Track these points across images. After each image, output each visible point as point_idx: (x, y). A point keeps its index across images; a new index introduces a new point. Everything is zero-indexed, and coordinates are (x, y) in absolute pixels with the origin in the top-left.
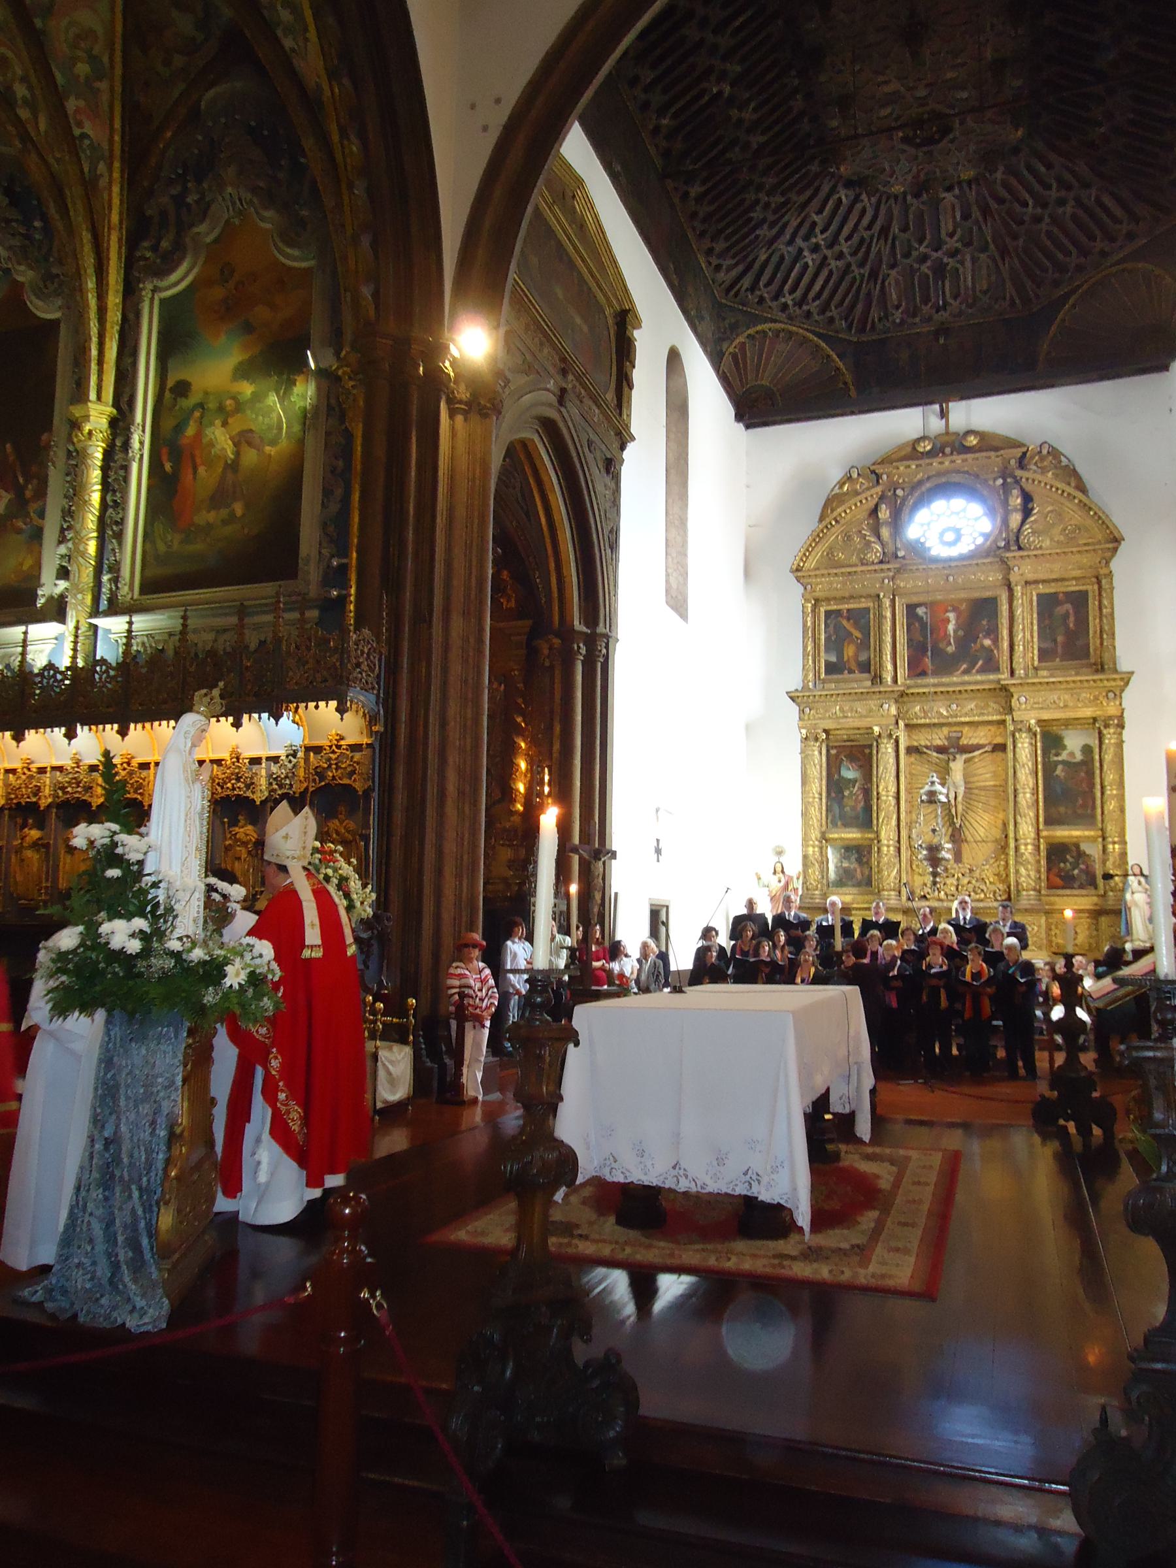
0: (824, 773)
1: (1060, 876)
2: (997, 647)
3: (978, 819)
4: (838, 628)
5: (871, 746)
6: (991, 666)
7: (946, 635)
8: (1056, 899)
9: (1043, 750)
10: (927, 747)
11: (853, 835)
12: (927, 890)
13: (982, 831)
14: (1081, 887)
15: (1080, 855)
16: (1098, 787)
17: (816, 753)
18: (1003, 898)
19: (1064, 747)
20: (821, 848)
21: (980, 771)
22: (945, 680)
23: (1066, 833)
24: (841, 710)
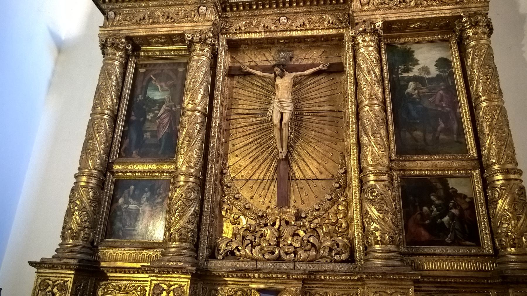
1: (426, 227)
5: (186, 64)
9: (390, 65)
10: (251, 67)
14: (455, 242)
15: (451, 195)
18: (343, 257)
19: (416, 62)
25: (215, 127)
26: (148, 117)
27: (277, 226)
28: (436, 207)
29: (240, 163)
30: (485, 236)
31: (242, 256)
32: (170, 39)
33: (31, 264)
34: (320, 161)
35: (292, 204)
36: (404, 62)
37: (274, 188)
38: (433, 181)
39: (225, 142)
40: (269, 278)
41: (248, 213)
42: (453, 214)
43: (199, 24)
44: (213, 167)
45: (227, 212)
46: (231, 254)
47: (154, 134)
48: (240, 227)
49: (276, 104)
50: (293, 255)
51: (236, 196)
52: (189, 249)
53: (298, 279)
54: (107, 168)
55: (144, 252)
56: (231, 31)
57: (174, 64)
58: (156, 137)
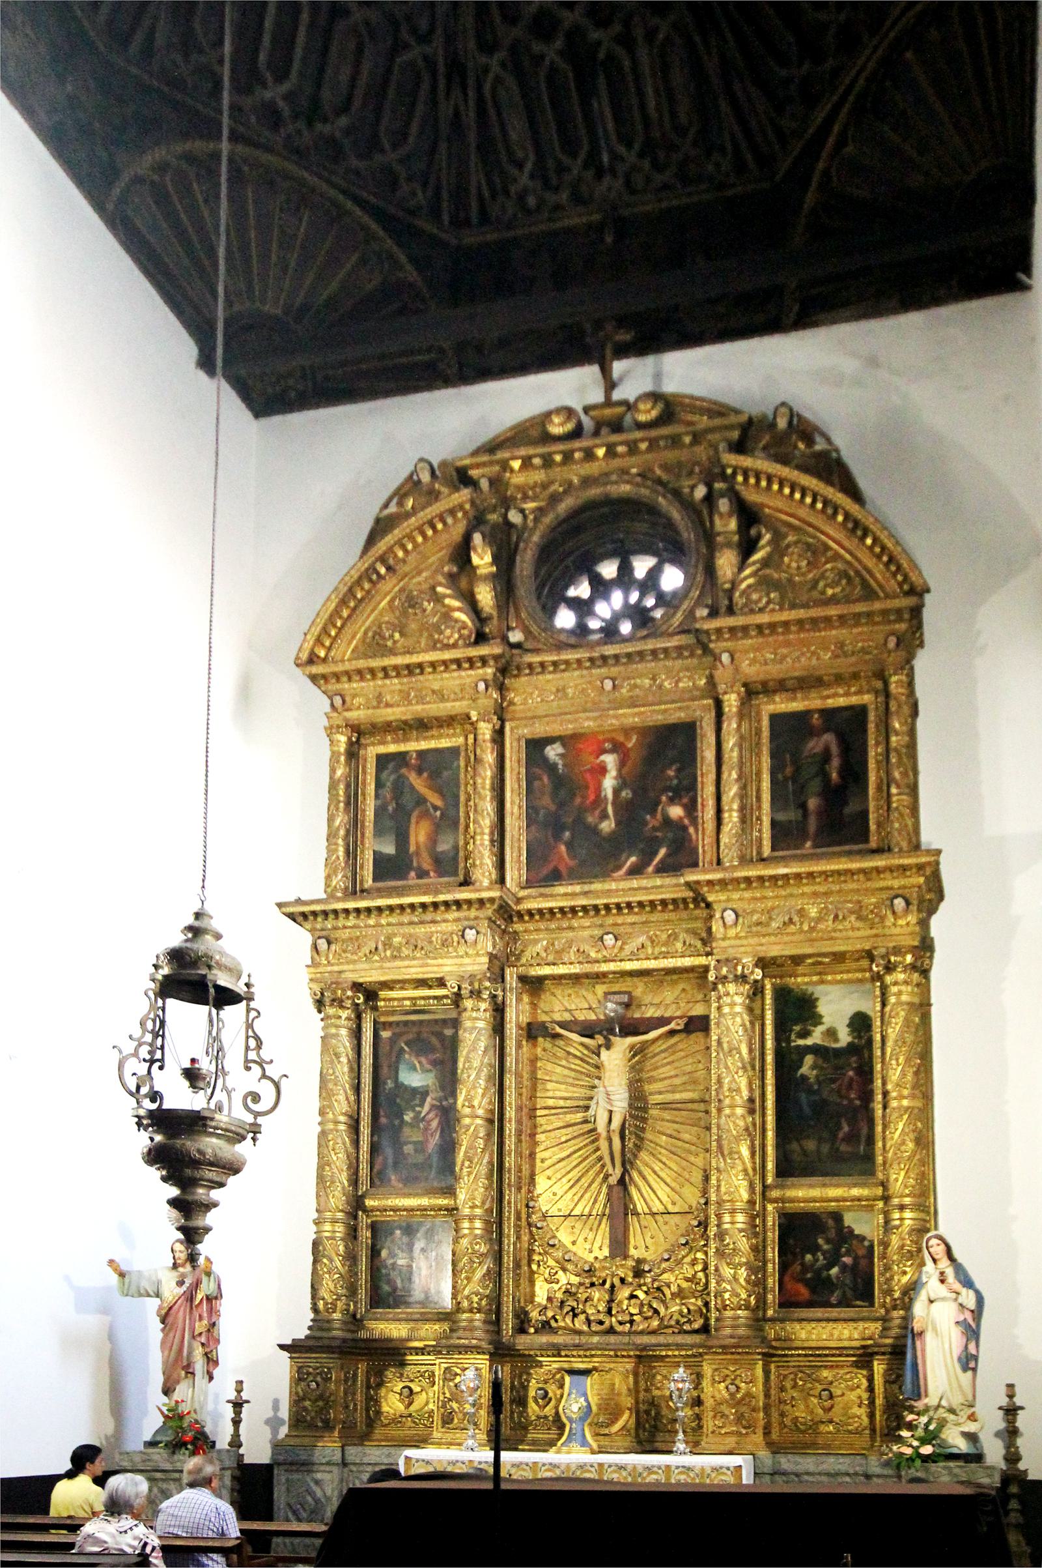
1: (807, 1283)
2: (694, 821)
4: (400, 787)
5: (456, 1023)
6: (682, 855)
7: (599, 800)
8: (797, 1326)
10: (562, 1025)
15: (845, 1236)
16: (879, 1097)
18: (696, 1326)
19: (817, 1019)
22: (597, 886)
23: (815, 1193)
25: (510, 1136)
26: (407, 1118)
27: (607, 1286)
28: (823, 1254)
29: (554, 1189)
31: (560, 1328)
34: (673, 1185)
35: (632, 1252)
37: (605, 1227)
38: (824, 1216)
39: (530, 1155)
40: (592, 1356)
41: (570, 1267)
42: (844, 1263)
45: (539, 1266)
46: (546, 1327)
47: (420, 1147)
50: (628, 1325)
51: (551, 1242)
53: (629, 1356)
54: (356, 1205)
55: (427, 1327)
57: (436, 1021)
58: (423, 1151)
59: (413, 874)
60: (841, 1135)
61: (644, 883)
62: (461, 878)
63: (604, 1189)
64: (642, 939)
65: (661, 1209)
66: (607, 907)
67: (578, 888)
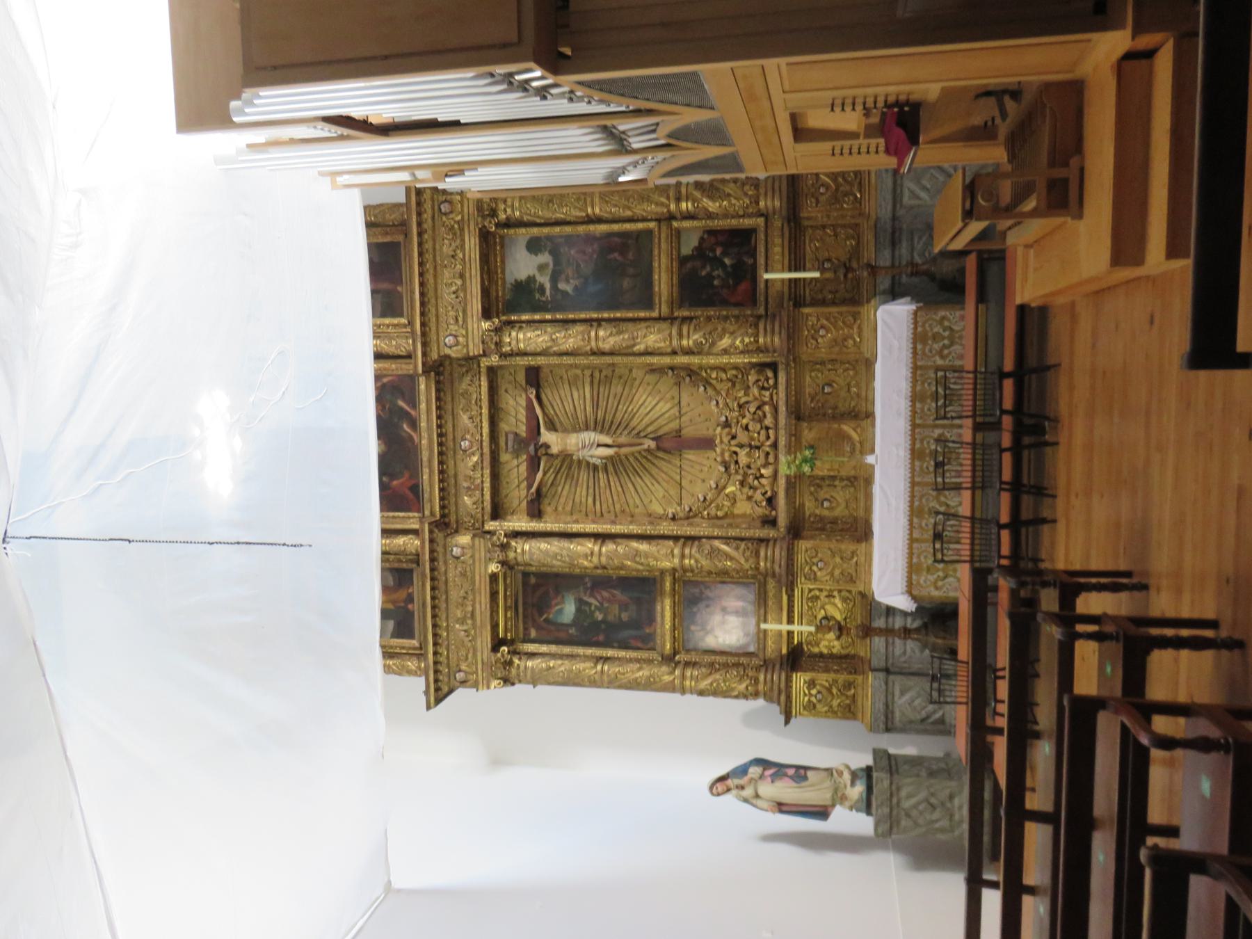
0: (567, 650)
3: (643, 411)
5: (526, 575)
10: (529, 487)
11: (665, 610)
12: (758, 496)
13: (663, 407)
14: (753, 253)
15: (700, 252)
16: (591, 228)
17: (530, 664)
18: (770, 374)
19: (531, 279)
20: (687, 664)
21: (569, 408)
22: (425, 455)
24: (462, 621)
27: (737, 449)
30: (747, 222)
31: (772, 490)
32: (494, 595)
33: (787, 722)
35: (711, 432)
36: (531, 292)
37: (690, 455)
43: (477, 556)
44: (665, 528)
46: (771, 501)
47: (624, 607)
48: (738, 493)
49: (585, 454)
52: (767, 546)
54: (669, 659)
56: (479, 516)
59: (410, 606)
60: (619, 258)
61: (424, 417)
62: (414, 566)
63: (660, 454)
64: (464, 418)
65: (676, 409)
66: (440, 444)
67: (426, 471)
